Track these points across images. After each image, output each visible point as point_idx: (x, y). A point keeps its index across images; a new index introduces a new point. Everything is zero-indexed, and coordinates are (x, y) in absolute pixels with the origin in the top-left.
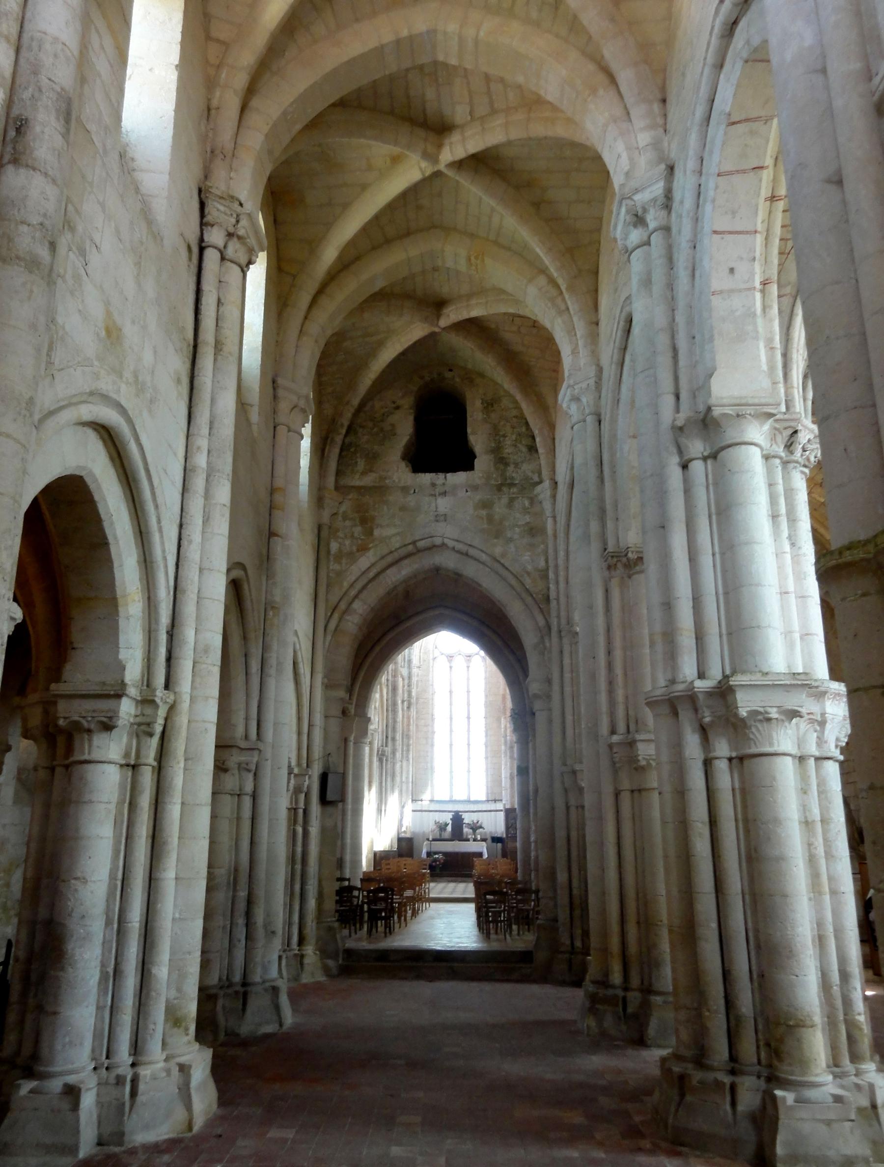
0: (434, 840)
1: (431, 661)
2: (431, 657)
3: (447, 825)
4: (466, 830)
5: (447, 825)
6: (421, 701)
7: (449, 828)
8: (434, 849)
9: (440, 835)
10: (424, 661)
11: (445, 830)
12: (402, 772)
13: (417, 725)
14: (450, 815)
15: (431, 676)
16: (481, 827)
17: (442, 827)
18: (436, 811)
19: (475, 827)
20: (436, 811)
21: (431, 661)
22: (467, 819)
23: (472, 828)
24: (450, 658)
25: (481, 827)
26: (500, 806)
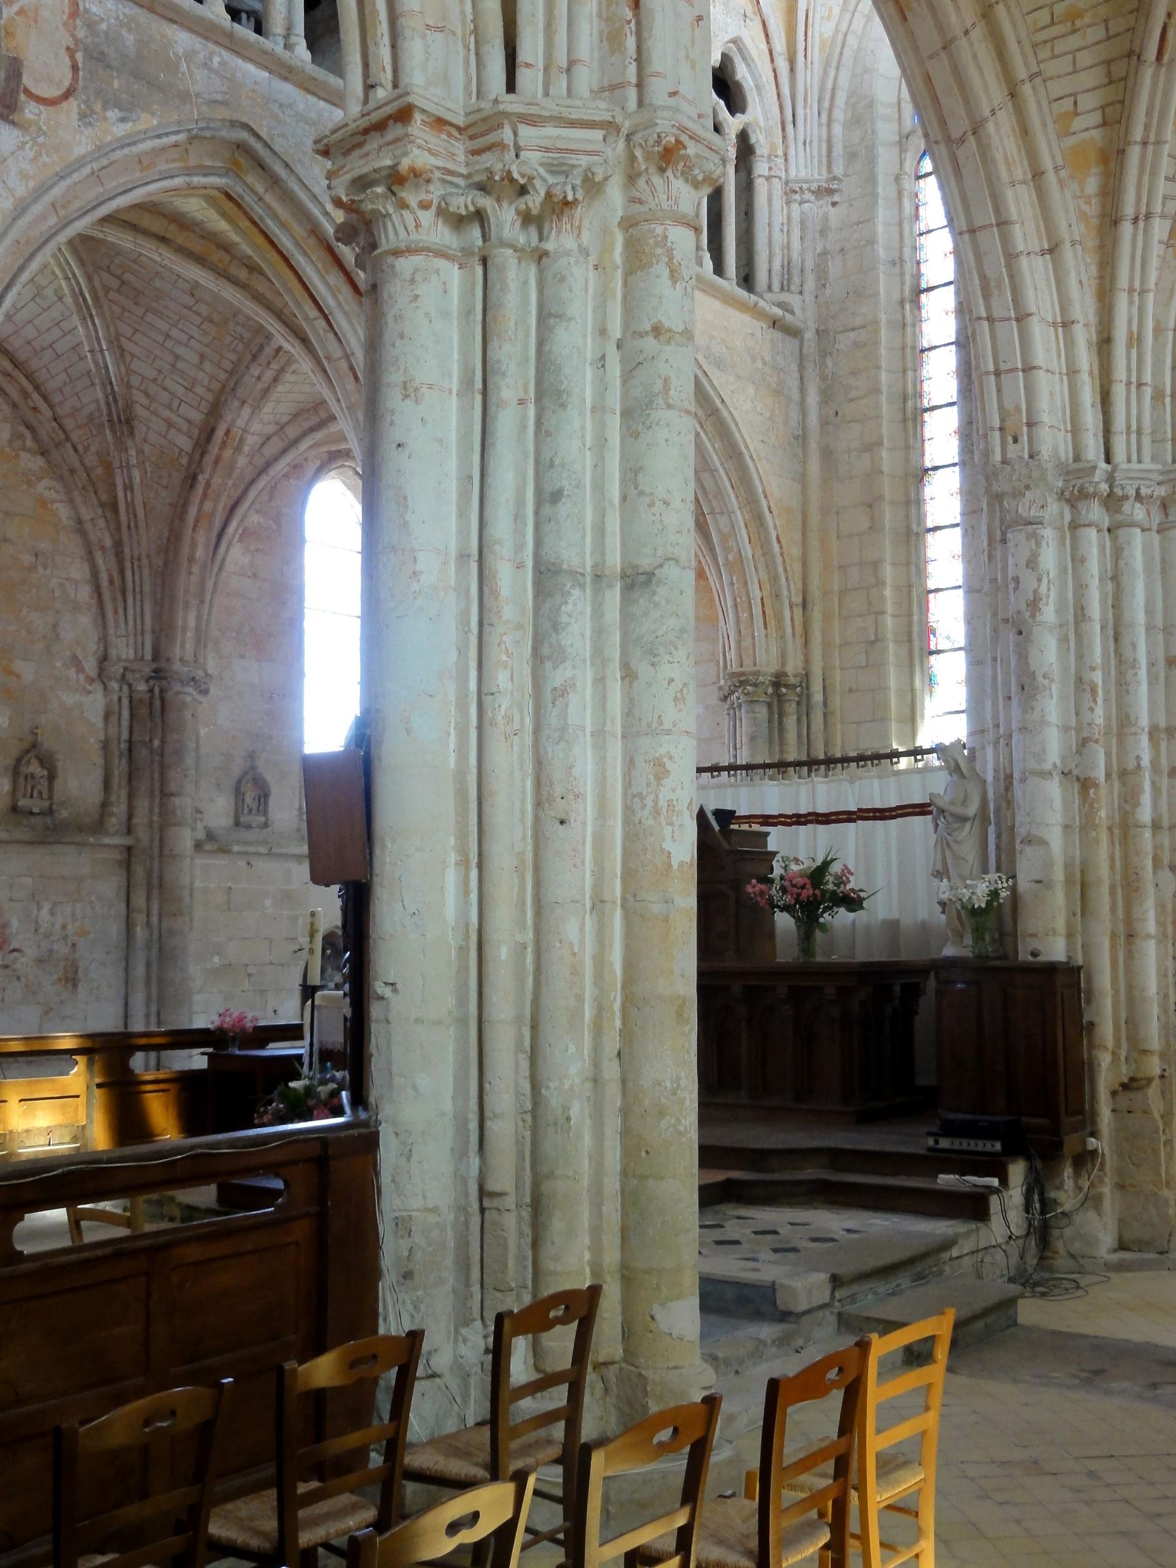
6: (845, 341)
10: (851, 156)
13: (827, 453)
16: (852, 902)
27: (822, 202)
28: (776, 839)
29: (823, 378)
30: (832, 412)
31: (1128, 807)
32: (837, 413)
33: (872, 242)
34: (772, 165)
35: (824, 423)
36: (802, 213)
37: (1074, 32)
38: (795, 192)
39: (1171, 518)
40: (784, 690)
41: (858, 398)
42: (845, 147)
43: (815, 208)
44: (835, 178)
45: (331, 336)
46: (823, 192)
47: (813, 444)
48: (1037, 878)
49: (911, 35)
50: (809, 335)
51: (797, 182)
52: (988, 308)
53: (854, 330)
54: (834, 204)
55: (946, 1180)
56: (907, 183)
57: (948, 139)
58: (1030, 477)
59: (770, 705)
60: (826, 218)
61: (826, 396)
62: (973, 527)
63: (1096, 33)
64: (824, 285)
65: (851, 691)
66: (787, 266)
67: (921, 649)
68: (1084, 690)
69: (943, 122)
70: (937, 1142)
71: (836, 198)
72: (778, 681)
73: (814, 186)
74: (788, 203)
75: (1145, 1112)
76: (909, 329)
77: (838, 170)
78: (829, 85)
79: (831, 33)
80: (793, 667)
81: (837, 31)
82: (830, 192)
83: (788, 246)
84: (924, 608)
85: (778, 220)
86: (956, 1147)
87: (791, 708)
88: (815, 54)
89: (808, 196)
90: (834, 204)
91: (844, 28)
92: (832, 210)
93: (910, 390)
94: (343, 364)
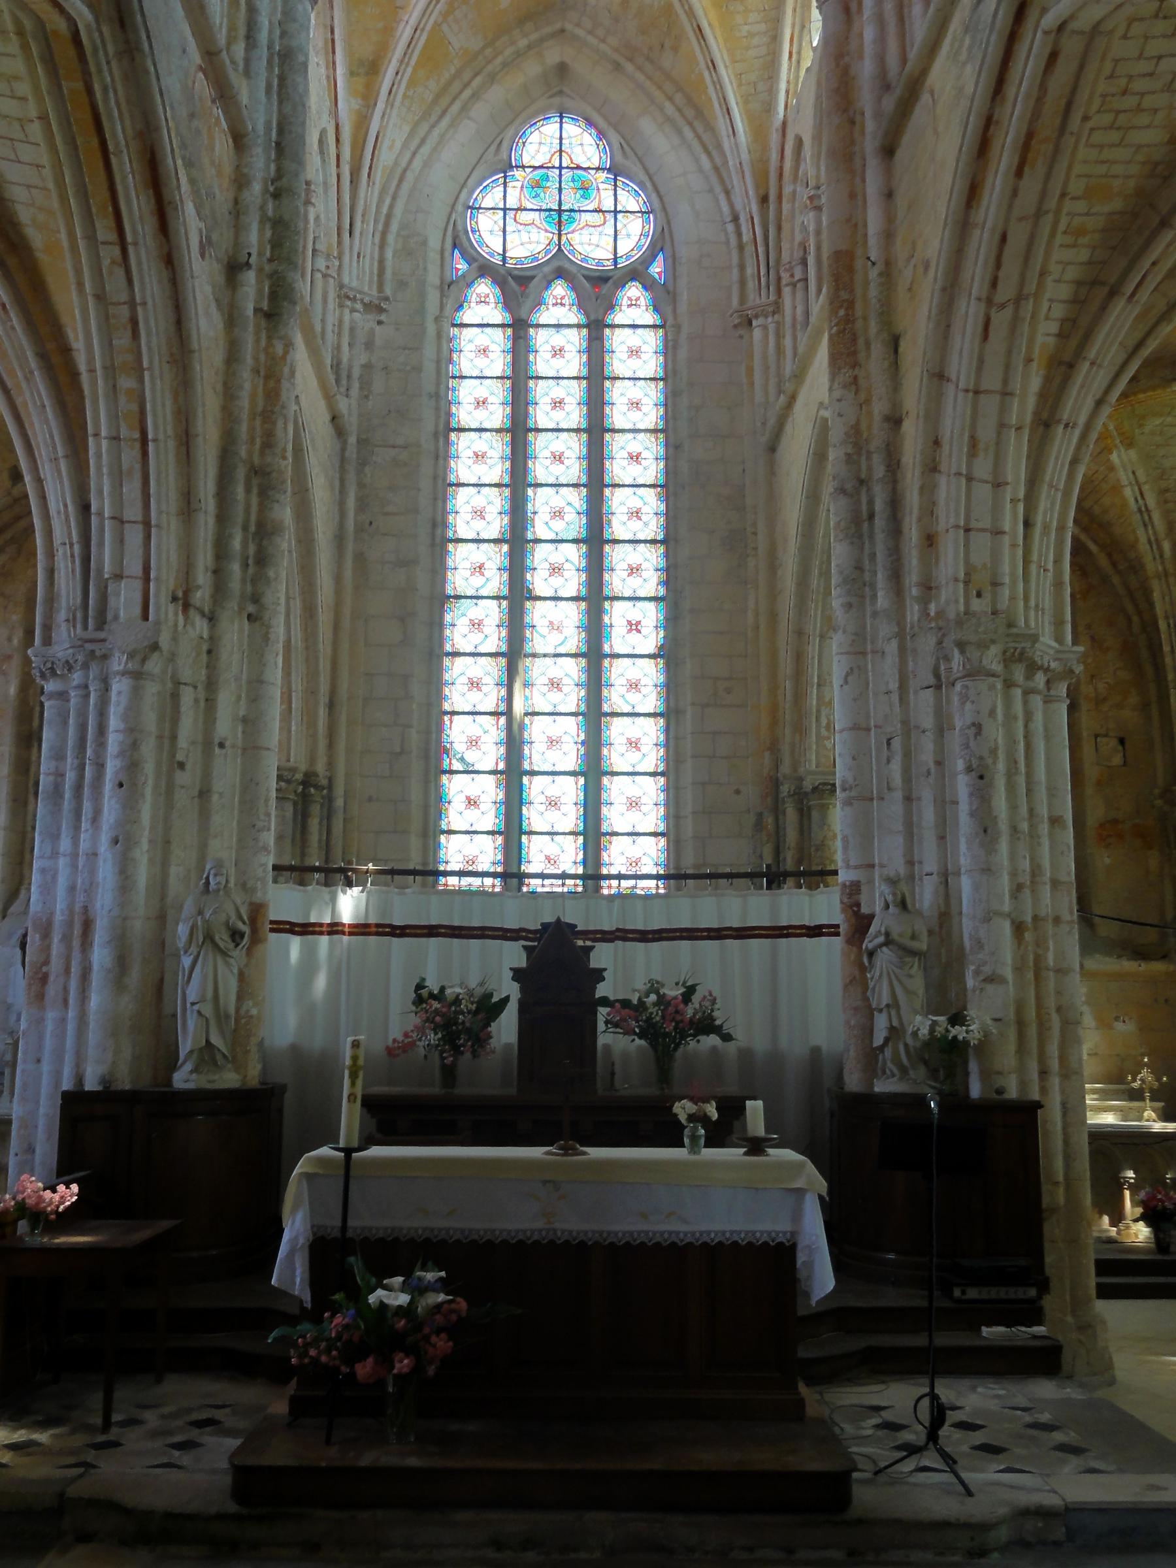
0: (392, 1117)
1: (433, 297)
2: (433, 278)
3: (490, 1008)
4: (605, 1038)
5: (490, 1008)
7: (506, 1029)
8: (368, 1219)
9: (449, 1074)
10: (402, 284)
11: (480, 1039)
12: (211, 685)
13: (360, 558)
14: (514, 955)
15: (429, 351)
17: (456, 1023)
18: (431, 931)
19: (671, 1025)
20: (431, 931)
21: (433, 297)
22: (622, 973)
23: (650, 1032)
24: (519, 287)
25: (706, 1025)
26: (824, 906)
27: (369, 317)
28: (602, 956)
29: (361, 485)
30: (368, 521)
31: (1040, 952)
32: (371, 523)
33: (418, 369)
34: (330, 264)
35: (359, 529)
36: (352, 321)
37: (1074, 246)
38: (348, 297)
39: (1052, 692)
40: (312, 790)
41: (394, 514)
42: (394, 274)
43: (364, 322)
44: (387, 299)
45: (120, 272)
46: (369, 307)
47: (350, 547)
48: (997, 1016)
49: (1015, 193)
50: (352, 440)
51: (351, 289)
52: (969, 465)
53: (394, 447)
54: (380, 323)
55: (992, 1333)
56: (446, 325)
57: (989, 302)
58: (995, 632)
59: (295, 804)
60: (372, 333)
61: (363, 504)
62: (859, 667)
63: (1084, 255)
64: (366, 397)
65: (370, 799)
66: (337, 366)
67: (436, 768)
68: (1019, 839)
69: (994, 284)
70: (963, 1293)
71: (383, 317)
72: (309, 780)
73: (367, 300)
74: (341, 306)
75: (1053, 1241)
76: (441, 462)
77: (388, 291)
78: (385, 210)
79: (390, 163)
80: (320, 768)
81: (396, 163)
82: (381, 310)
83: (338, 347)
84: (440, 729)
85: (331, 320)
86: (985, 1296)
87: (315, 809)
88: (378, 176)
89: (359, 306)
90: (380, 323)
91: (403, 164)
92: (378, 328)
93: (439, 519)
94: (125, 311)
